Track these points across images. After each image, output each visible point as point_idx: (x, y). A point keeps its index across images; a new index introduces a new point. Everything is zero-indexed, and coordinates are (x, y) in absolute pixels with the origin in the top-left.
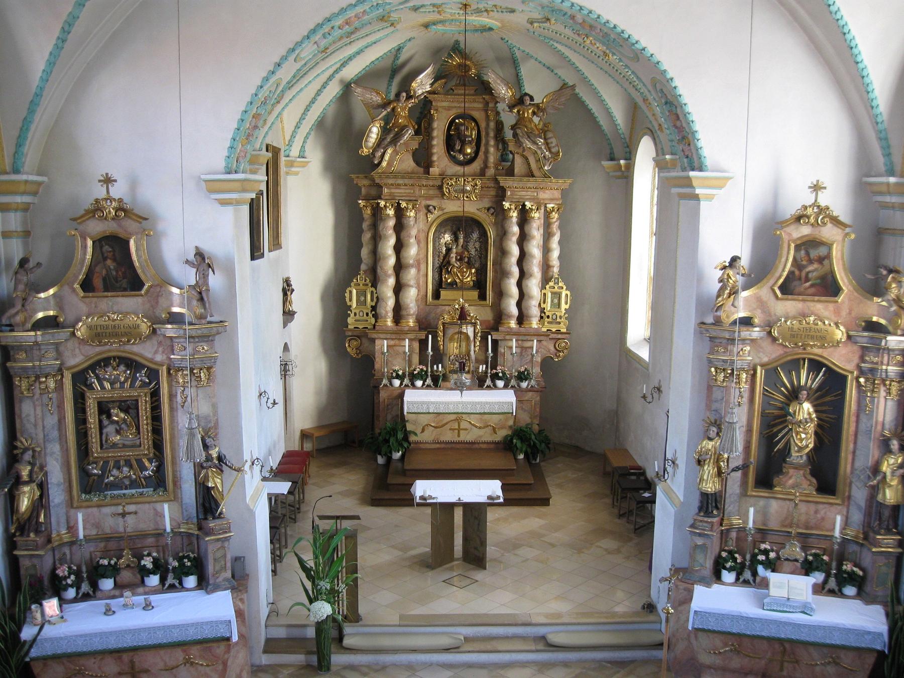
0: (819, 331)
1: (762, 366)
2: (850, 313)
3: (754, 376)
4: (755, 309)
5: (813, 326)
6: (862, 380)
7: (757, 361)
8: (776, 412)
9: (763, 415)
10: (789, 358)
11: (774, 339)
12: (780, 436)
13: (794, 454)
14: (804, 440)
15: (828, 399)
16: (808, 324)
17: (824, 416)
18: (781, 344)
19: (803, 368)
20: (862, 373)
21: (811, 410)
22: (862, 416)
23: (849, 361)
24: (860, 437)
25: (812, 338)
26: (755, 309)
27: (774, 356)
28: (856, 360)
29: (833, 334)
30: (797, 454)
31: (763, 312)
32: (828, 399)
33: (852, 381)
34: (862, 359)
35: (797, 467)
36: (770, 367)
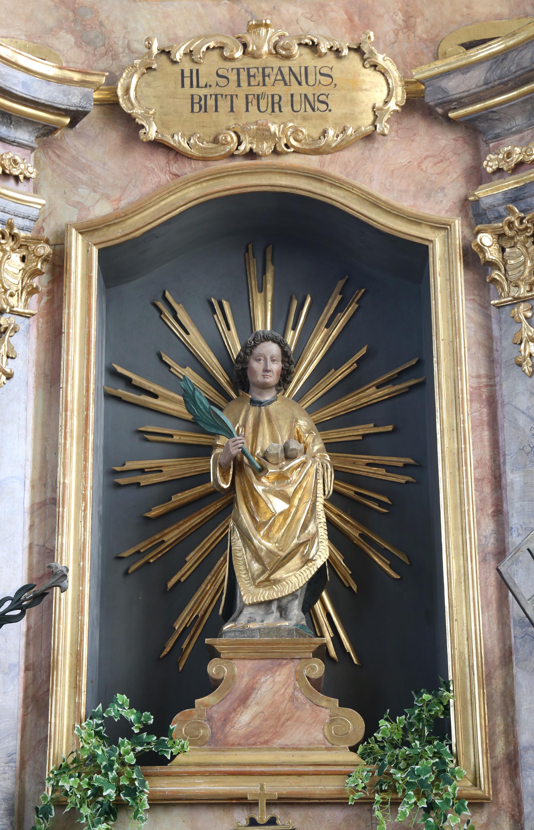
0: (301, 77)
1: (87, 230)
2: (408, 26)
3: (57, 266)
4: (51, 31)
5: (276, 63)
6: (486, 239)
7: (68, 215)
8: (174, 467)
9: (115, 480)
10: (194, 193)
11: (130, 126)
12: (193, 558)
13: (248, 593)
14: (289, 521)
15: (371, 394)
16: (254, 56)
17: (359, 465)
18: (158, 145)
19: (262, 289)
20: (476, 214)
21: (303, 423)
22: (505, 389)
23: (427, 191)
24: (513, 478)
25: (275, 104)
26: (51, 31)
27: (133, 195)
28: (453, 188)
29: (355, 85)
30: (264, 594)
31: (83, 41)
32: (371, 394)
33: (449, 261)
34: (477, 176)
35: (270, 651)
36: (115, 234)
